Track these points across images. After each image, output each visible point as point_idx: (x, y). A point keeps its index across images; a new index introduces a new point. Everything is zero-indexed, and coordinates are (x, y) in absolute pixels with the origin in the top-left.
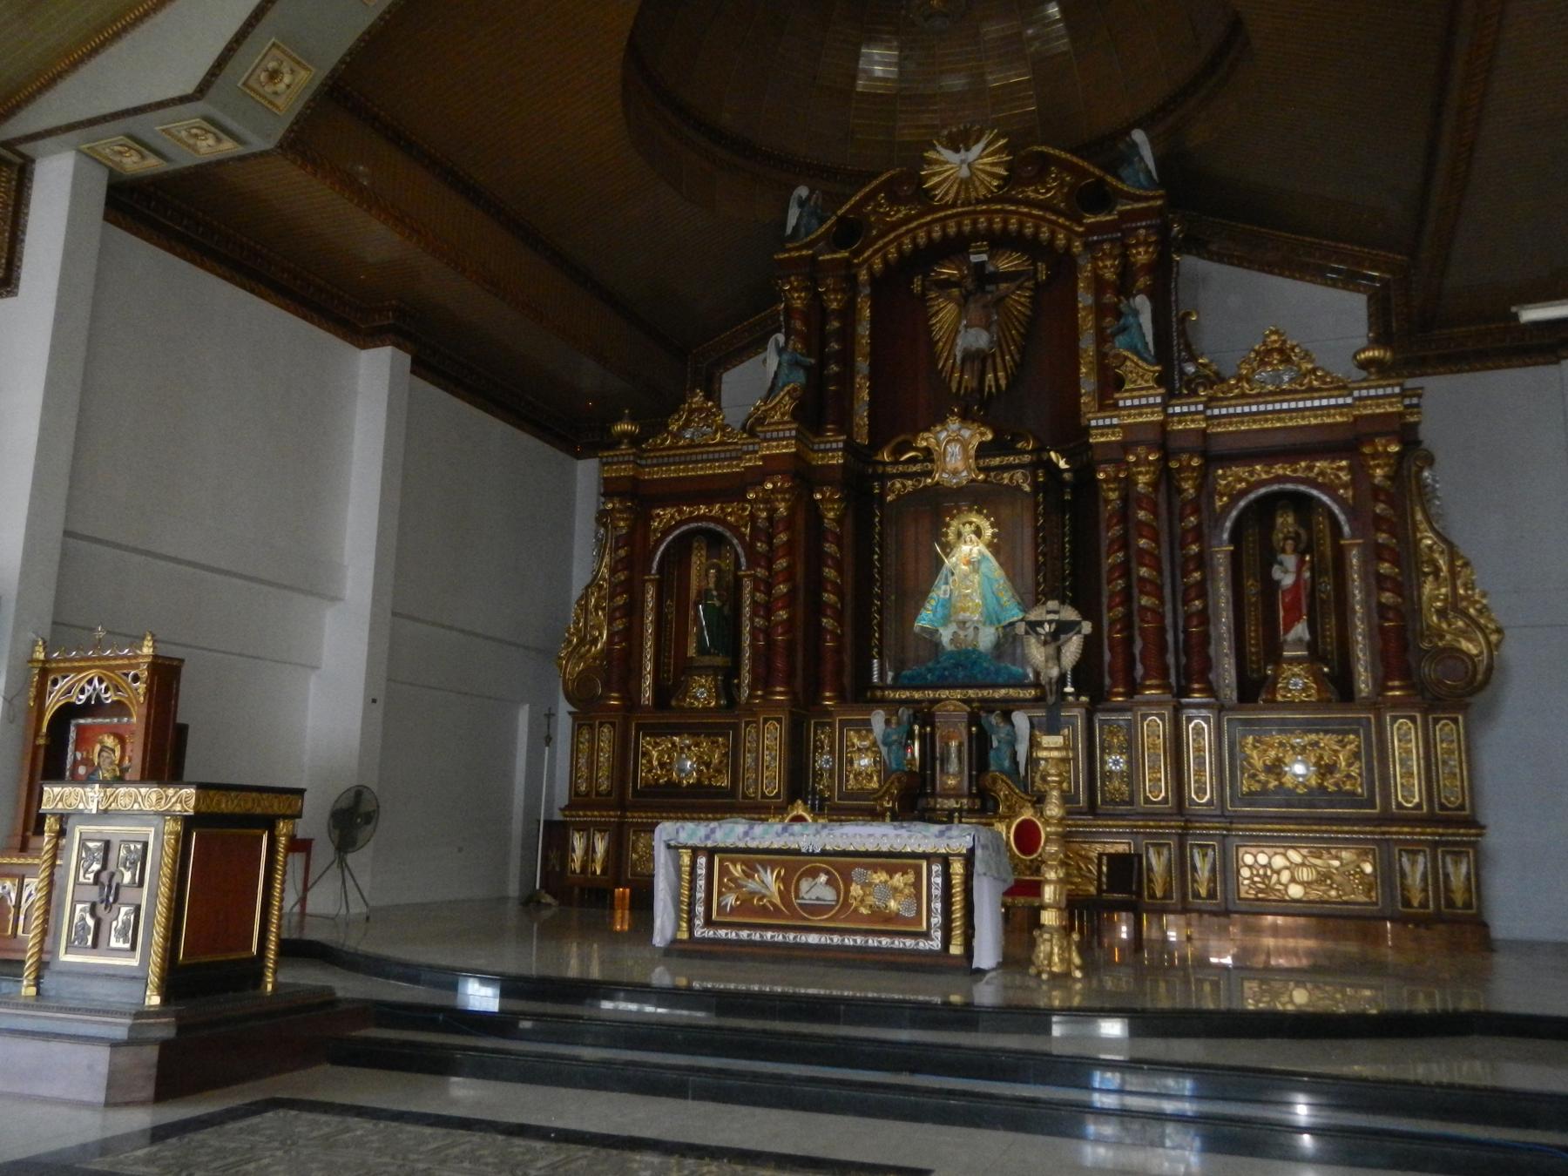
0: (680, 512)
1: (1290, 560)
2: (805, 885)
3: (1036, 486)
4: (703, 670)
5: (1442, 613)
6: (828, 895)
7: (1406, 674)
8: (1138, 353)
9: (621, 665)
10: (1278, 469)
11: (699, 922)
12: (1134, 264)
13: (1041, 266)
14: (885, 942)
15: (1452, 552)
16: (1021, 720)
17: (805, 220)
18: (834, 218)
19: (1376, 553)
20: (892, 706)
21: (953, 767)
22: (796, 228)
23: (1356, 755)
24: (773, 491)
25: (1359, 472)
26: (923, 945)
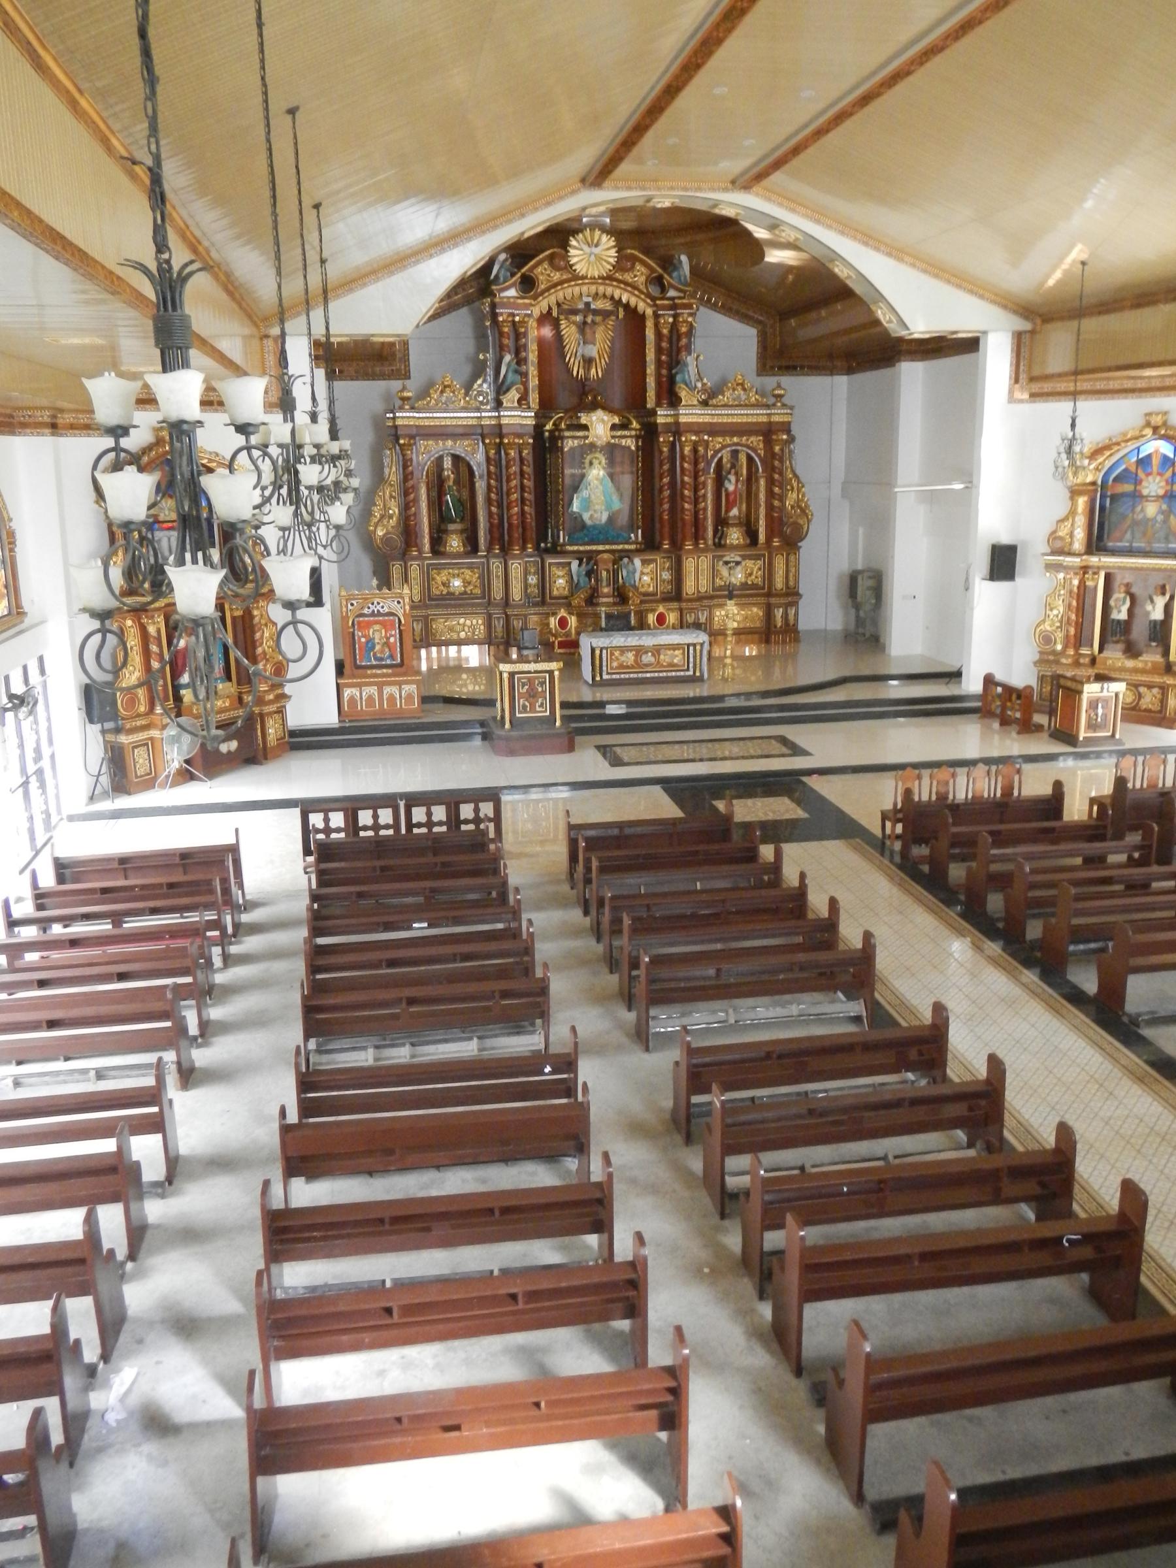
0: (437, 444)
1: (733, 478)
2: (644, 657)
3: (637, 447)
4: (453, 532)
5: (792, 507)
6: (652, 660)
7: (781, 535)
8: (686, 385)
9: (408, 532)
10: (735, 439)
11: (604, 673)
12: (678, 331)
13: (621, 310)
14: (674, 674)
15: (799, 482)
16: (637, 562)
17: (503, 272)
18: (519, 275)
19: (771, 482)
20: (580, 558)
21: (604, 583)
22: (497, 276)
23: (760, 569)
24: (509, 443)
25: (768, 443)
26: (687, 673)
